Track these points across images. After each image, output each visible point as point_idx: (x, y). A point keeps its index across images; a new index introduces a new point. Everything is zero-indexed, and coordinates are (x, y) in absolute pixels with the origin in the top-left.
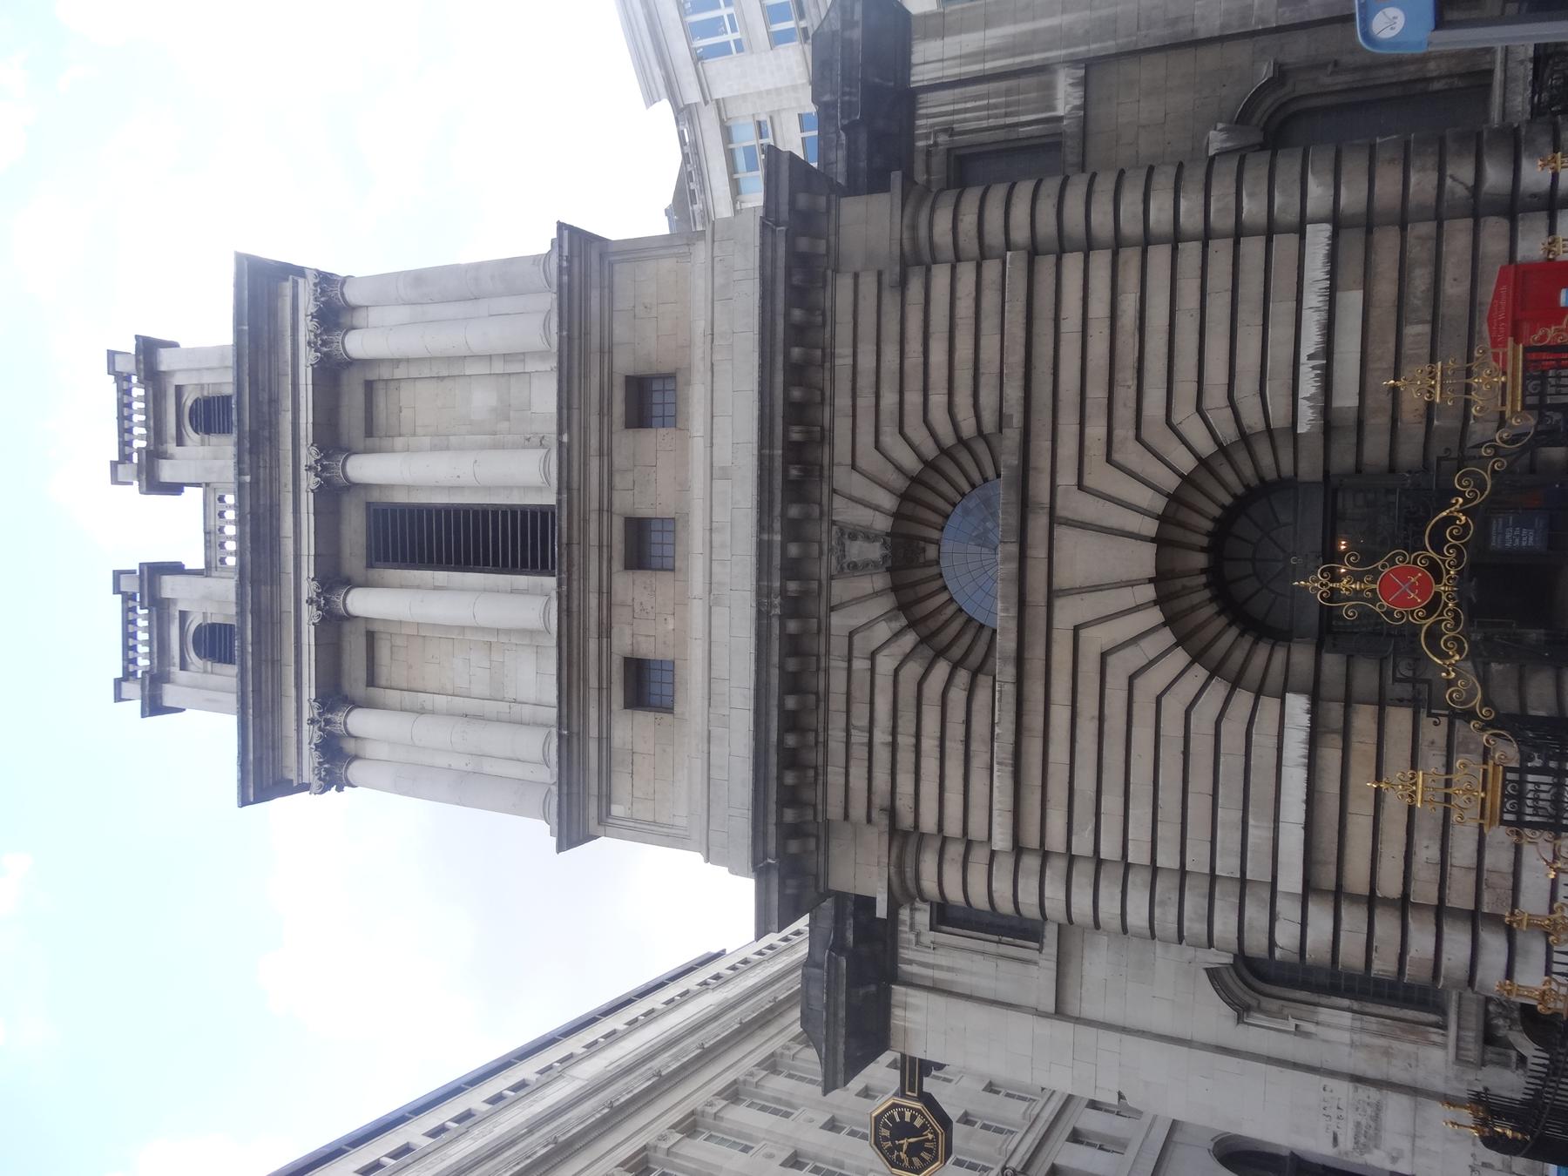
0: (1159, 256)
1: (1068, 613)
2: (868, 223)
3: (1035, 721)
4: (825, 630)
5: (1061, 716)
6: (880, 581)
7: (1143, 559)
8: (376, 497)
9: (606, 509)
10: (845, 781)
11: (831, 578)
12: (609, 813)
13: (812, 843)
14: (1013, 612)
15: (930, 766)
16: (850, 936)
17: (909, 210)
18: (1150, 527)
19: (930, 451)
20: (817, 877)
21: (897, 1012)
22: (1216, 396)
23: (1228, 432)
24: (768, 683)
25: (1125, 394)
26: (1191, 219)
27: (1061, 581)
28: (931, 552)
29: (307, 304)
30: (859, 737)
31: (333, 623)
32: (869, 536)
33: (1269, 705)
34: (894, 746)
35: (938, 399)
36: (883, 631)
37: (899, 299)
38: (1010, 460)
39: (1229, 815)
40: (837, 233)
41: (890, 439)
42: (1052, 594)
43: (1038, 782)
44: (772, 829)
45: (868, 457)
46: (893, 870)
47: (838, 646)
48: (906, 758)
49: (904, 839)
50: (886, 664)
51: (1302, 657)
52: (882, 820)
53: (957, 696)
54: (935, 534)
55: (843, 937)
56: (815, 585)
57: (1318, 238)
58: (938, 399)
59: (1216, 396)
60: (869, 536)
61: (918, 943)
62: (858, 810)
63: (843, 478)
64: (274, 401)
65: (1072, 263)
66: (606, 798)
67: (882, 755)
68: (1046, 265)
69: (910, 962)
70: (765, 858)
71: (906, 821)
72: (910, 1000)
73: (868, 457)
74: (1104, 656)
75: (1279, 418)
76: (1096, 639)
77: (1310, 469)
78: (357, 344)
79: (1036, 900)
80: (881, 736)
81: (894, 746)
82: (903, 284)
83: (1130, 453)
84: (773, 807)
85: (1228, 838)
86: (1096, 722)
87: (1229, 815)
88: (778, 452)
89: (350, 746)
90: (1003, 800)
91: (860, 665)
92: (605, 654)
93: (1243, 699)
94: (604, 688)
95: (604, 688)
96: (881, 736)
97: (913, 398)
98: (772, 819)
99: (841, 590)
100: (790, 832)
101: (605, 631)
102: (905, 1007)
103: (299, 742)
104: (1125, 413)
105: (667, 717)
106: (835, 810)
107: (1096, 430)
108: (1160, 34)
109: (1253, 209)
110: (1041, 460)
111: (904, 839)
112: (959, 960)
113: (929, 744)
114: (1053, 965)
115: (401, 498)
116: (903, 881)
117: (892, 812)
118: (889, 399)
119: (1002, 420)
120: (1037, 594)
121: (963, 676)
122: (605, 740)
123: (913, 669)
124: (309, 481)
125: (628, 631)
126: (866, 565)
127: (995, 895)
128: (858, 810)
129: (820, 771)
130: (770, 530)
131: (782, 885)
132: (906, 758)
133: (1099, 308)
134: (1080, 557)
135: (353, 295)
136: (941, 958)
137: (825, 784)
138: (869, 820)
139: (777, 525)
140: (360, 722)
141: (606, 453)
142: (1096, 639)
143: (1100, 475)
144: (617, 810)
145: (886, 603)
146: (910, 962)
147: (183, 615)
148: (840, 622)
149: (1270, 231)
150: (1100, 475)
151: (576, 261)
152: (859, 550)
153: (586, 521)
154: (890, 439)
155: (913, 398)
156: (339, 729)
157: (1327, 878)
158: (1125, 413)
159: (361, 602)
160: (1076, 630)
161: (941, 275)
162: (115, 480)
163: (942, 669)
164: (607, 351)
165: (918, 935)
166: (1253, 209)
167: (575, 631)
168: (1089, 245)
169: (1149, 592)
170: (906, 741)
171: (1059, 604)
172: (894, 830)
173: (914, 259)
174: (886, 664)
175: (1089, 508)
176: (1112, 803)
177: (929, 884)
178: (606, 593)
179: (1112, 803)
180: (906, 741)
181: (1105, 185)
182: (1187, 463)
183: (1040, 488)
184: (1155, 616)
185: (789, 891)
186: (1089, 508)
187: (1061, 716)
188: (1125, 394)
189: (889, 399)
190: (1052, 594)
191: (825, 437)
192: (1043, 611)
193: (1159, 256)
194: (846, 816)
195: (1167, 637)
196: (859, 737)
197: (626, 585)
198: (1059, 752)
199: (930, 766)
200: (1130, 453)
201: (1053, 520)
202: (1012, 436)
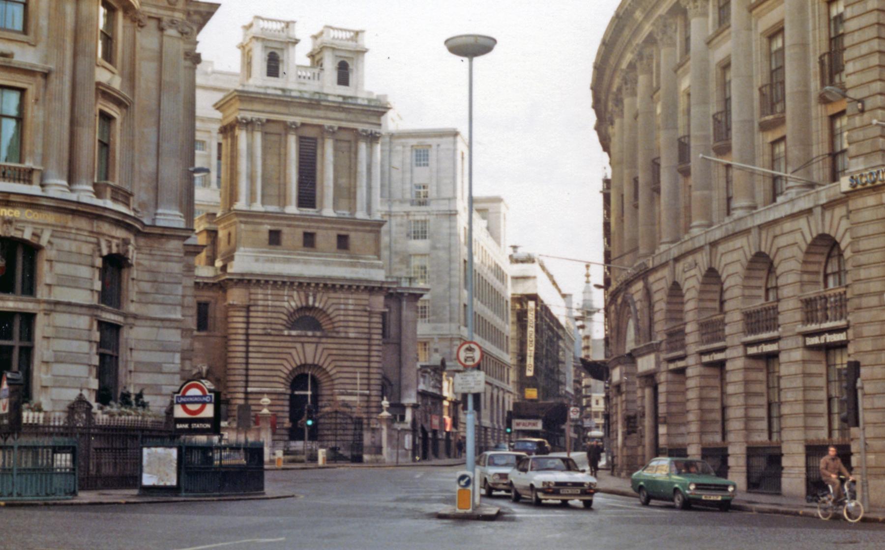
0: (366, 364)
1: (298, 346)
2: (378, 302)
4: (294, 290)
6: (304, 304)
7: (310, 361)
8: (319, 141)
9: (318, 228)
10: (259, 294)
18: (316, 363)
19: (332, 316)
22: (338, 375)
23: (333, 377)
25: (342, 358)
26: (372, 370)
27: (306, 345)
29: (374, 129)
31: (288, 128)
32: (314, 301)
33: (282, 386)
36: (293, 304)
38: (330, 334)
39: (261, 379)
41: (334, 307)
42: (303, 343)
45: (331, 301)
47: (290, 293)
49: (248, 308)
50: (286, 304)
51: (289, 392)
52: (252, 302)
53: (280, 321)
57: (367, 392)
58: (342, 318)
59: (338, 375)
62: (253, 297)
64: (350, 112)
65: (366, 347)
66: (246, 223)
68: (366, 342)
71: (252, 308)
73: (331, 301)
74: (290, 354)
75: (336, 387)
76: (293, 352)
77: (325, 392)
78: (363, 147)
82: (366, 311)
83: (329, 359)
85: (256, 378)
87: (261, 379)
89: (250, 127)
90: (260, 332)
92: (282, 225)
93: (283, 381)
94: (273, 225)
95: (273, 225)
99: (302, 293)
100: (249, 281)
101: (289, 226)
103: (252, 111)
104: (337, 358)
105: (267, 242)
106: (253, 291)
107: (334, 352)
108: (403, 360)
109: (373, 382)
110: (330, 340)
111: (248, 308)
115: (319, 152)
119: (338, 332)
120: (303, 339)
121: (285, 323)
123: (285, 311)
124: (327, 123)
128: (253, 297)
133: (358, 353)
134: (310, 349)
138: (250, 300)
141: (332, 228)
142: (293, 352)
143: (326, 353)
145: (299, 305)
147: (282, 49)
149: (369, 385)
150: (326, 353)
152: (311, 299)
154: (334, 307)
156: (256, 128)
157: (250, 396)
158: (337, 358)
161: (367, 319)
163: (285, 318)
164: (356, 230)
166: (373, 382)
168: (369, 350)
169: (303, 362)
173: (370, 314)
175: (319, 351)
177: (237, 314)
178: (298, 226)
179: (260, 355)
181: (380, 354)
182: (328, 369)
183: (324, 340)
184: (299, 363)
186: (319, 351)
188: (342, 358)
190: (303, 343)
191: (335, 292)
193: (366, 364)
195: (294, 366)
197: (299, 232)
198: (270, 344)
200: (329, 359)
201: (317, 343)
202: (334, 335)
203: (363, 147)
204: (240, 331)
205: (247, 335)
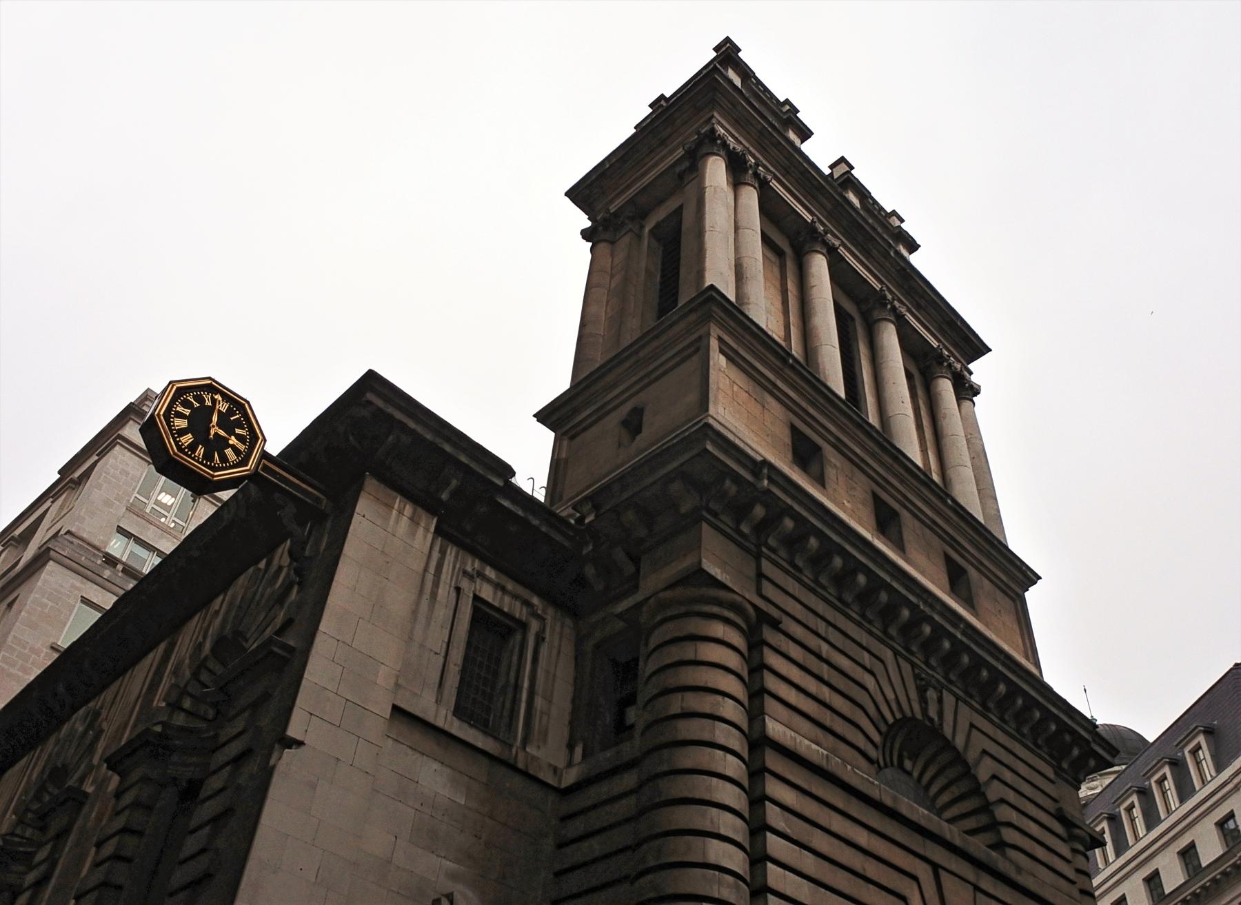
3: (856, 808)
5: (862, 838)
10: (788, 595)
11: (913, 665)
12: (721, 351)
13: (745, 528)
14: (923, 823)
15: (812, 685)
16: (506, 503)
17: (1088, 839)
20: (715, 515)
21: (408, 510)
24: (881, 567)
28: (908, 764)
30: (821, 627)
34: (819, 657)
35: (1014, 817)
37: (1052, 811)
40: (1066, 781)
42: (936, 867)
43: (814, 791)
44: (789, 501)
46: (739, 599)
48: (812, 663)
50: (869, 681)
53: (860, 741)
54: (916, 774)
55: (506, 497)
56: (914, 649)
58: (1014, 817)
60: (941, 714)
61: (465, 572)
63: (964, 709)
66: (733, 358)
67: (812, 642)
69: (443, 553)
70: (769, 478)
72: (421, 531)
79: (721, 740)
80: (825, 649)
81: (819, 657)
82: (1061, 817)
84: (805, 514)
86: (861, 871)
88: (1000, 668)
91: (866, 659)
96: (825, 649)
97: (1011, 796)
98: (797, 507)
99: (906, 667)
101: (839, 446)
102: (414, 520)
112: (442, 613)
113: (825, 693)
114: (440, 723)
116: (719, 603)
117: (775, 625)
118: (1008, 776)
122: (772, 390)
123: (872, 710)
125: (838, 464)
126: (926, 703)
127: (719, 698)
128: (769, 590)
129: (794, 571)
130: (964, 633)
131: (737, 478)
132: (812, 663)
135: (967, 404)
136: (445, 592)
137: (787, 572)
139: (964, 639)
140: (750, 197)
144: (722, 360)
146: (443, 553)
148: (888, 655)
151: (1021, 576)
153: (902, 482)
155: (1011, 796)
159: (819, 266)
160: (915, 878)
161: (1064, 849)
162: (842, 160)
165: (471, 578)
167: (845, 421)
170: (825, 671)
171: (928, 868)
172: (764, 618)
174: (869, 681)
176: (808, 863)
177: (719, 630)
180: (825, 671)
185: (728, 483)
187: (862, 838)
189: (1008, 776)
190: (936, 867)
191: (984, 712)
192: (921, 851)
194: (760, 575)
196: (821, 627)
199: (812, 685)
203: (946, 387)
204: (729, 709)
205: (759, 742)
